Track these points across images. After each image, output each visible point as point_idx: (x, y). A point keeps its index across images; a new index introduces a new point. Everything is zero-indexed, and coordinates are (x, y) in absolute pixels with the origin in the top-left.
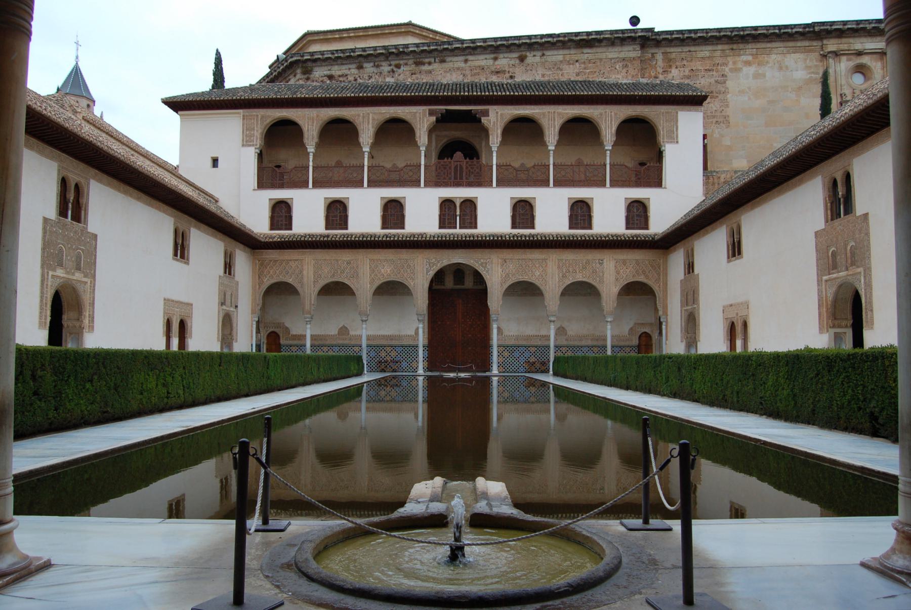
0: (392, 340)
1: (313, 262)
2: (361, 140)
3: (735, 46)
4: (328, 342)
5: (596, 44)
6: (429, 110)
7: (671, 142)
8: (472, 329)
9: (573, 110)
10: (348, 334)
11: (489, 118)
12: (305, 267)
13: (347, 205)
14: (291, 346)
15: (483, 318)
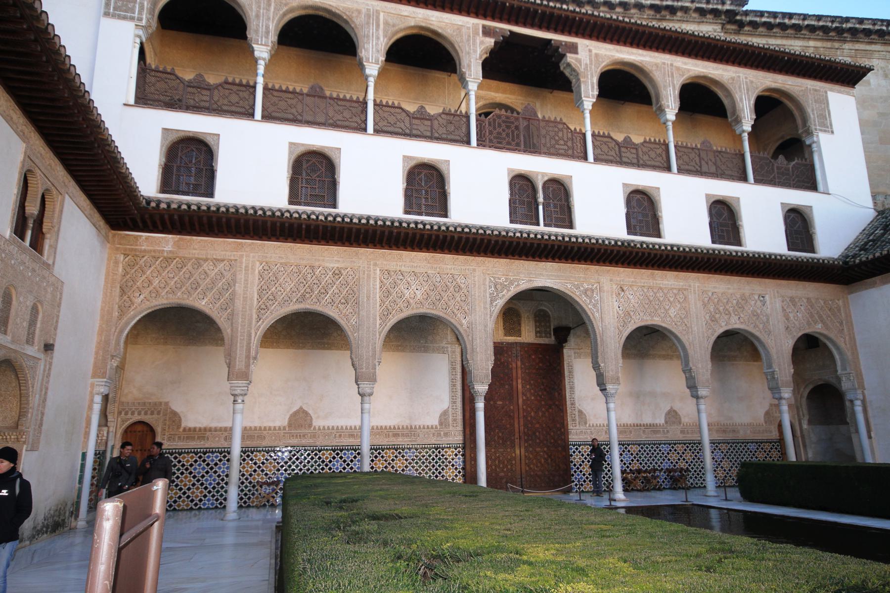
0: (396, 435)
1: (258, 267)
2: (362, 53)
3: (829, 44)
4: (264, 443)
5: (668, 17)
6: (484, 27)
7: (825, 131)
8: (540, 414)
9: (696, 65)
10: (310, 425)
11: (579, 56)
12: (241, 277)
13: (336, 161)
14: (180, 454)
15: (556, 394)
